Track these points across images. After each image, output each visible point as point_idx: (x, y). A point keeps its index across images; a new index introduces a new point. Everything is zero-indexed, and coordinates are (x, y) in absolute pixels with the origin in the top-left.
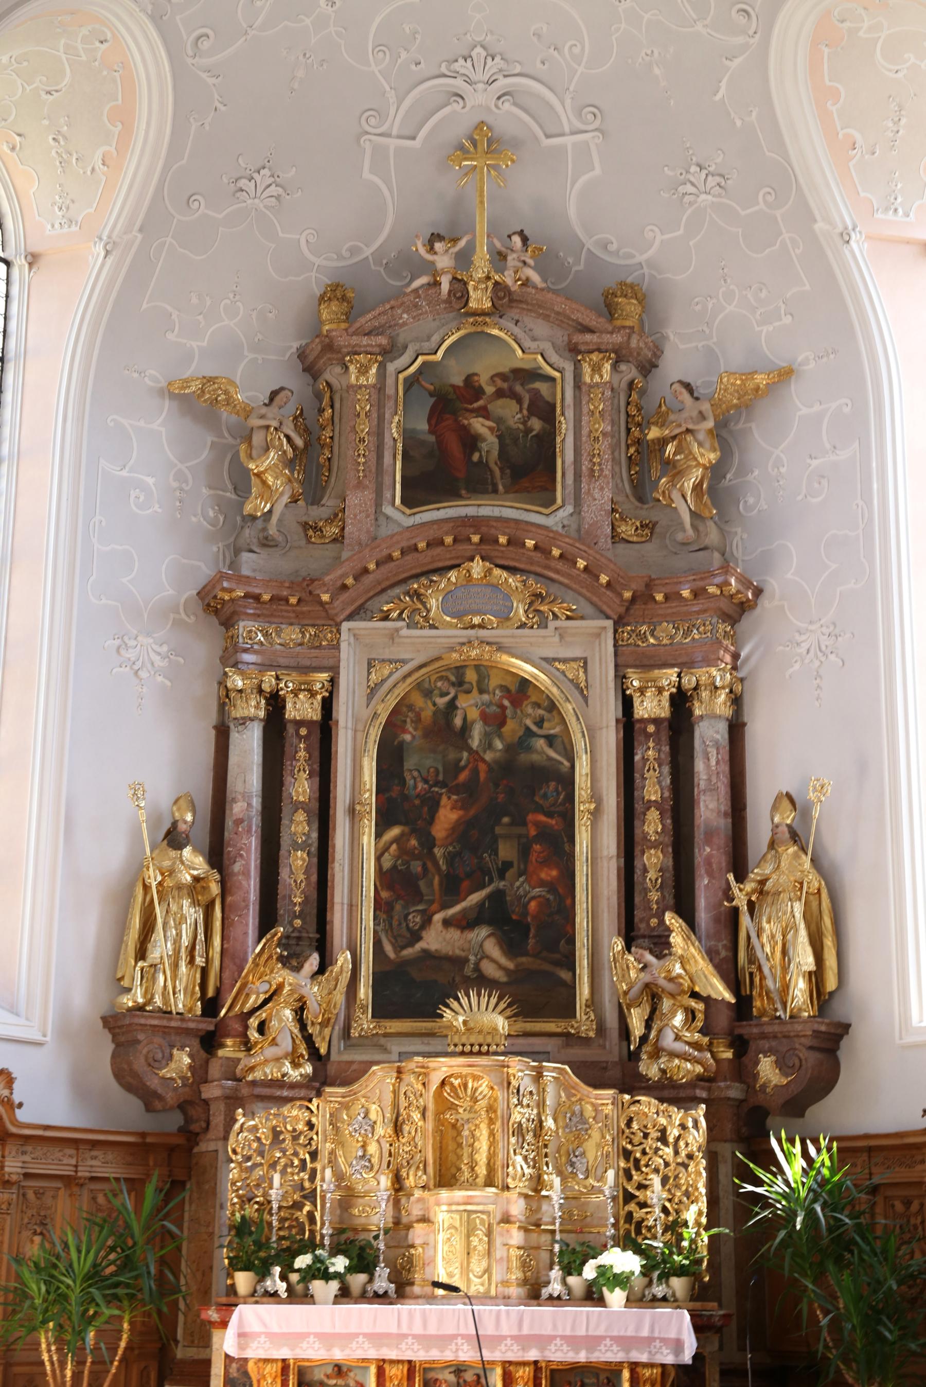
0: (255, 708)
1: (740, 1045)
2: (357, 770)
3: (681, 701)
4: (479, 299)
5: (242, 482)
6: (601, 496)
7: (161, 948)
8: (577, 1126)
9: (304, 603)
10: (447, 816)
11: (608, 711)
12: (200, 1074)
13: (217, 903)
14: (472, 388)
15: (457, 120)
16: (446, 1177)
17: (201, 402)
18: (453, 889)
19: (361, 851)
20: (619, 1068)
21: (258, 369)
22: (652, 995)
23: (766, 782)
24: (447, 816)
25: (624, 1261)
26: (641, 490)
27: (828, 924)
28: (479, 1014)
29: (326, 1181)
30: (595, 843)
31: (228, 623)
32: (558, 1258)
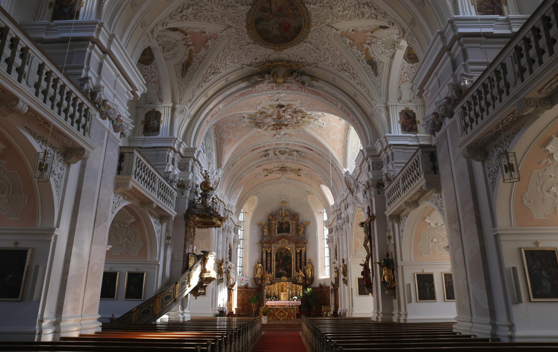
0: (265, 252)
1: (305, 280)
2: (274, 257)
3: (301, 251)
4: (284, 215)
5: (263, 232)
6: (294, 233)
7: (258, 272)
8: (292, 287)
9: (269, 242)
10: (281, 261)
11: (295, 252)
12: (261, 282)
13: (262, 269)
14: (283, 223)
15: (282, 200)
16: (282, 291)
17: (260, 225)
18: (282, 267)
19: (274, 264)
20: (295, 282)
21: (264, 222)
22: (298, 276)
23: (307, 259)
24: (281, 261)
25: (296, 298)
26: (297, 232)
27: (312, 270)
28: (284, 278)
29: (273, 292)
30: (293, 263)
31: (262, 244)
32: (290, 297)
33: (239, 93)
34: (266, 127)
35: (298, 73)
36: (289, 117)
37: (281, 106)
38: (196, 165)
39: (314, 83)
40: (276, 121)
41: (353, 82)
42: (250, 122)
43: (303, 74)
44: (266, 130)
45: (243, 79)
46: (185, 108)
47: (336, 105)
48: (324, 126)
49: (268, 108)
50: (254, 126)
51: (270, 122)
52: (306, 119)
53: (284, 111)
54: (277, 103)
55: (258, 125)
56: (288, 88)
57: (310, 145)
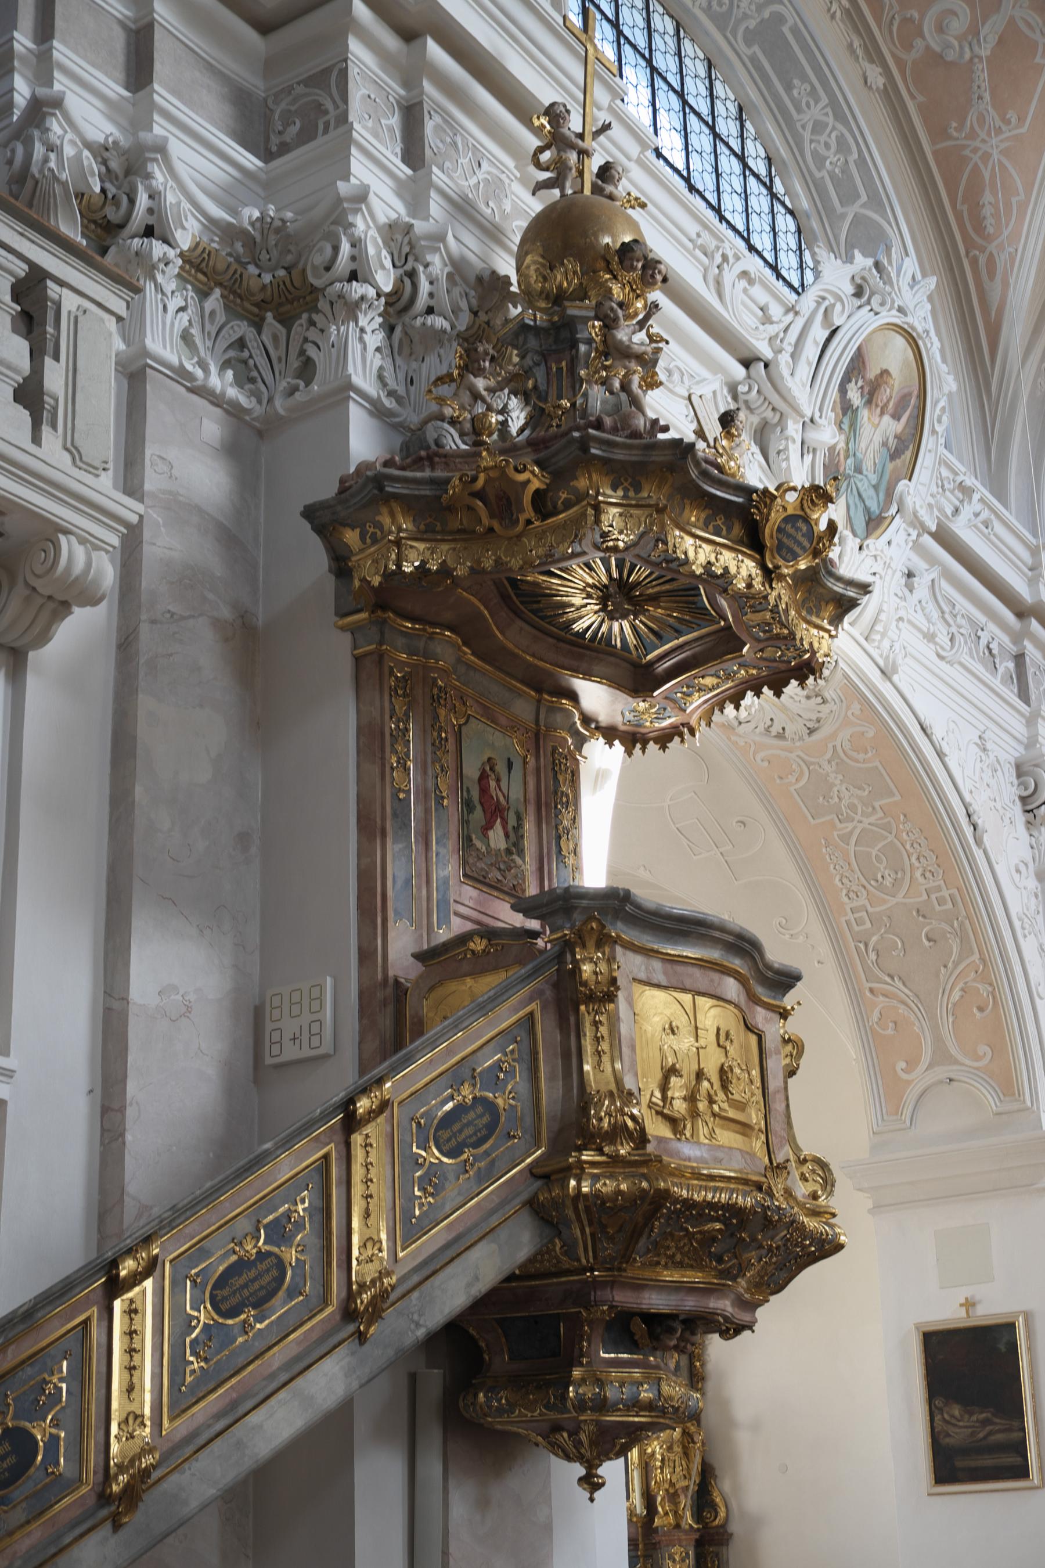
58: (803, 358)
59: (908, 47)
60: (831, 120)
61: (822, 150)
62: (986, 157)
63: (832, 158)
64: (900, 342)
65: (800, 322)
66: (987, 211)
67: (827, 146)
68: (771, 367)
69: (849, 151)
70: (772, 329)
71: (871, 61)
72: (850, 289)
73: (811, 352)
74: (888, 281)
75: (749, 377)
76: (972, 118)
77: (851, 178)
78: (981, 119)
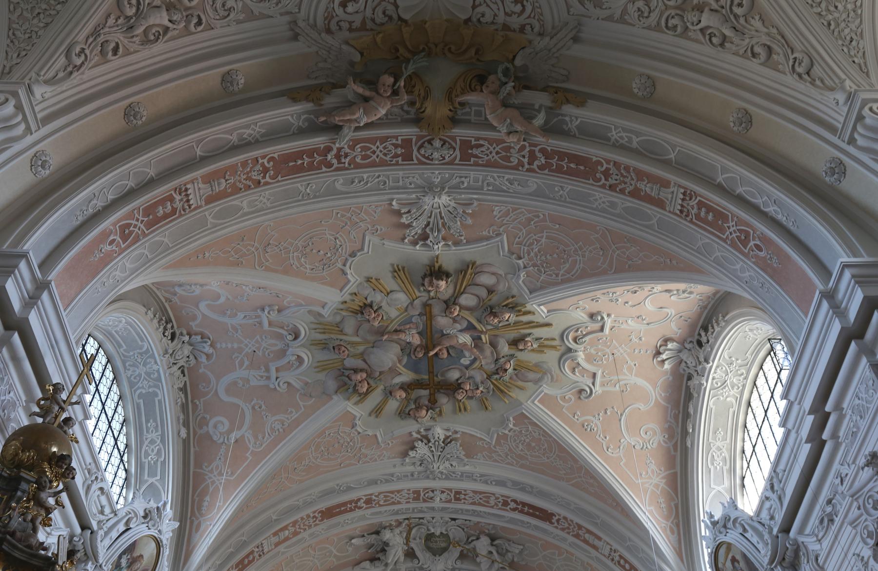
33: (277, 150)
34: (376, 397)
35: (506, 72)
36: (465, 339)
37: (436, 272)
38: (15, 358)
39: (569, 109)
40: (413, 366)
41: (729, 62)
42: (322, 367)
43: (525, 83)
44: (377, 411)
45: (294, 96)
46: (15, 95)
47: (660, 204)
48: (598, 389)
49: (389, 283)
50: (332, 384)
51: (393, 372)
52: (527, 356)
53: (449, 304)
54: (420, 254)
55: (348, 380)
56: (467, 153)
57: (541, 494)
58: (109, 536)
59: (201, 428)
60: (159, 441)
61: (150, 452)
62: (213, 482)
63: (153, 456)
64: (153, 545)
65: (116, 519)
66: (206, 504)
67: (153, 451)
68: (94, 535)
69: (161, 457)
70: (102, 517)
71: (184, 426)
72: (142, 514)
73: (114, 534)
74: (160, 517)
75: (81, 535)
76: (214, 465)
77: (156, 468)
78: (217, 467)
